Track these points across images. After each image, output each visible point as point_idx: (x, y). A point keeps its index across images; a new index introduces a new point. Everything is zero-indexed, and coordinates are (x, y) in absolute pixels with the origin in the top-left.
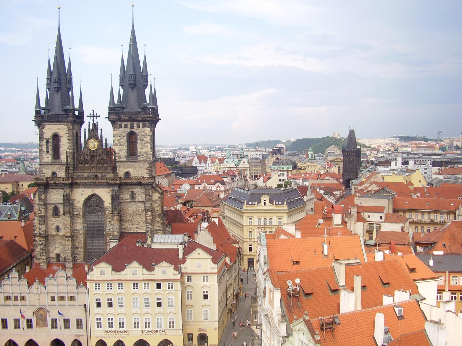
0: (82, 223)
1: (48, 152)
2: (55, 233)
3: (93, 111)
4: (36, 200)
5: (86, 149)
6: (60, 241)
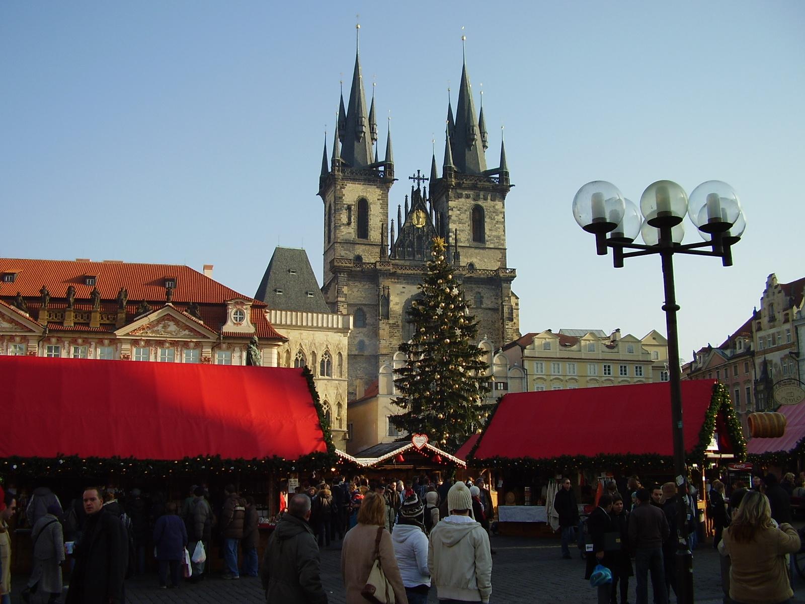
0: (401, 337)
1: (349, 224)
2: (356, 353)
3: (419, 171)
4: (328, 298)
6: (364, 365)
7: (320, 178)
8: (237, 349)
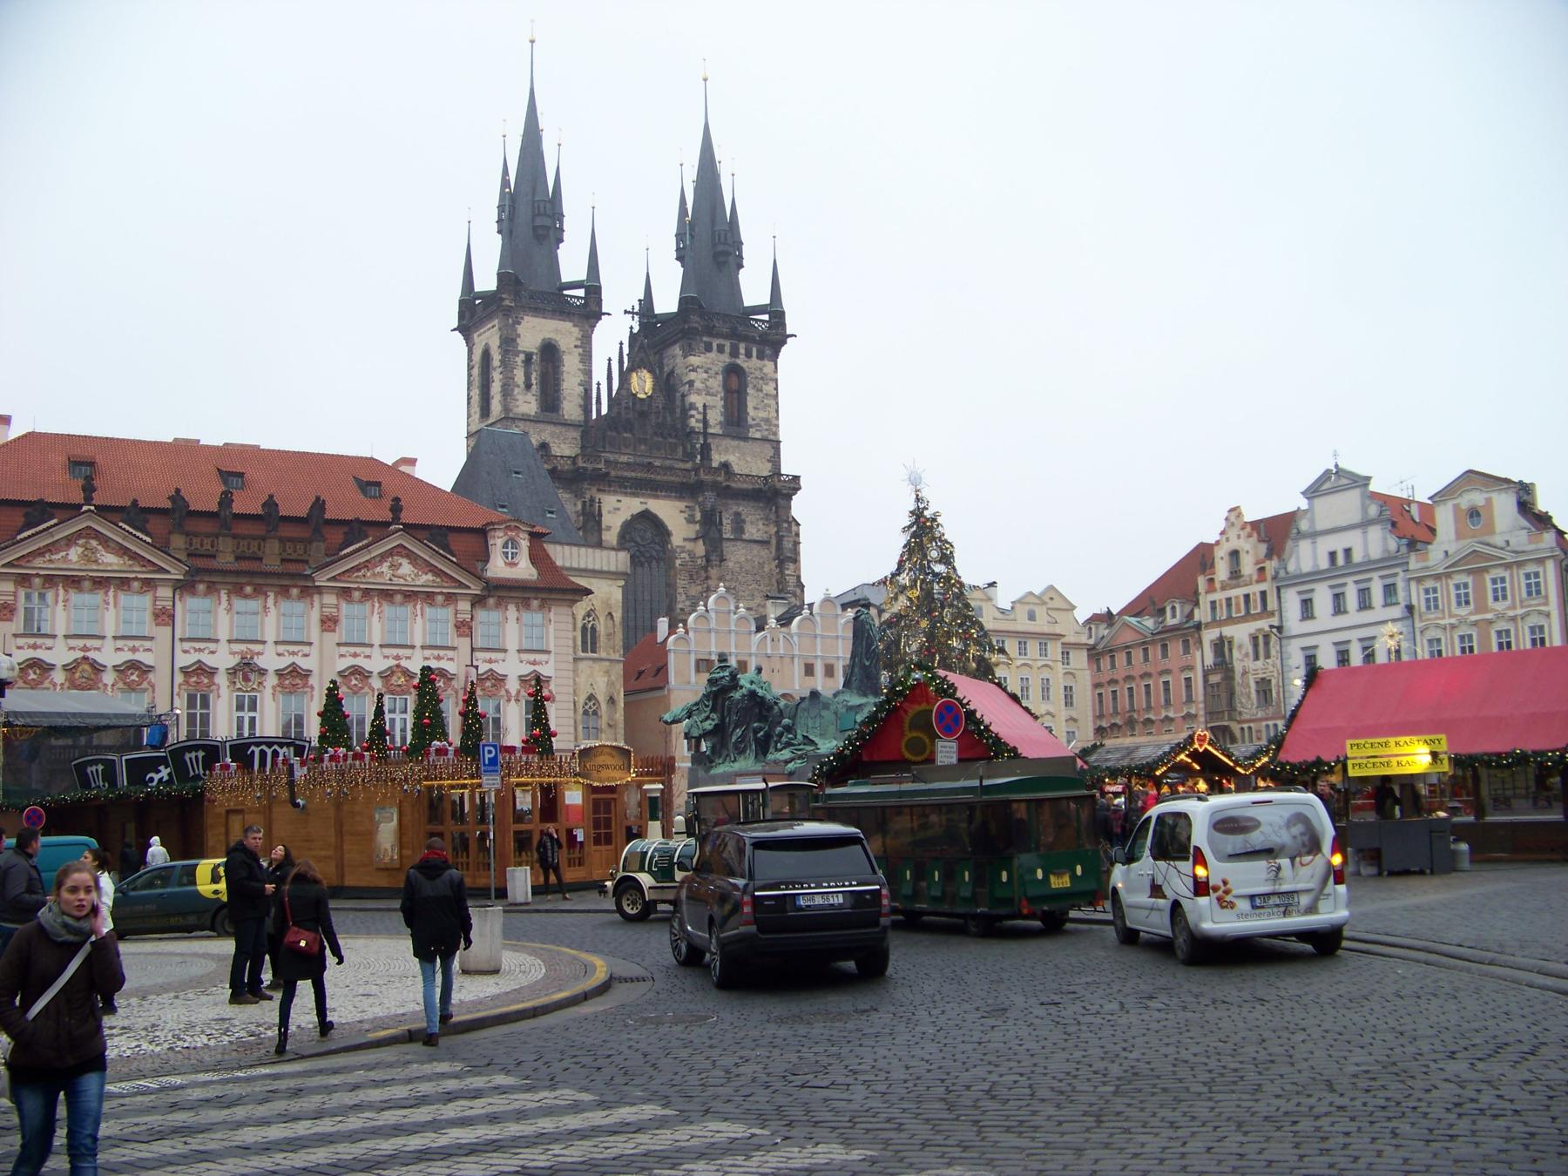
5: (624, 392)
7: (461, 302)
8: (512, 609)
